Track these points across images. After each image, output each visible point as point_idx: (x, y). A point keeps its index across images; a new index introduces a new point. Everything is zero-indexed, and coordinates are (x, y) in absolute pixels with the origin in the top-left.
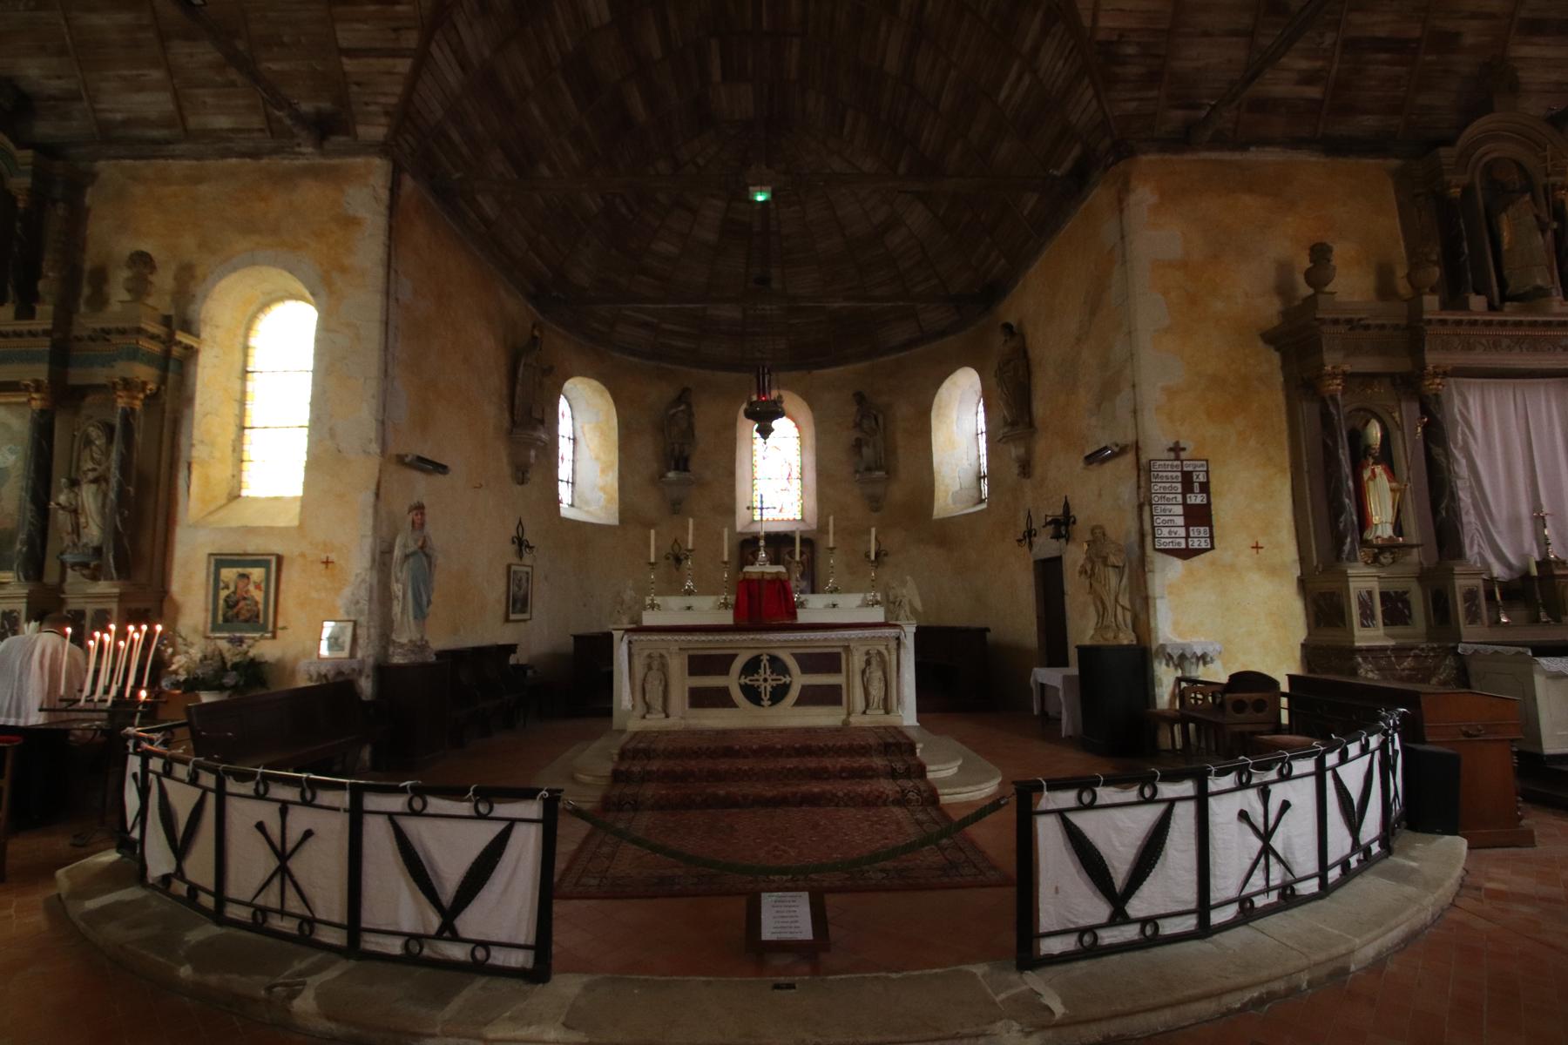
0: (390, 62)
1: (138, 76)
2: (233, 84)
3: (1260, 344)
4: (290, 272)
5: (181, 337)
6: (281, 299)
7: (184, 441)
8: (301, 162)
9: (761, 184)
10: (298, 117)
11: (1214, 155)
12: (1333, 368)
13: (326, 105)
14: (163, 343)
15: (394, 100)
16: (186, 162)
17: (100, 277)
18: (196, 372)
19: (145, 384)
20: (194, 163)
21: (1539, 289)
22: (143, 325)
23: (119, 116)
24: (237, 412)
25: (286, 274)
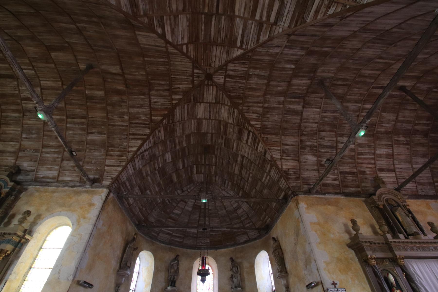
0: (117, 168)
2: (75, 171)
3: (347, 248)
4: (69, 218)
5: (27, 237)
6: (63, 225)
7: (9, 272)
8: (85, 189)
9: (205, 198)
10: (89, 179)
11: (318, 196)
12: (371, 256)
13: (97, 176)
14: (20, 238)
15: (115, 176)
16: (54, 188)
17: (13, 216)
18: (25, 248)
19: (7, 251)
20: (56, 188)
21: (415, 232)
22: (17, 233)
23: (42, 176)
24: (31, 262)
25: (67, 218)
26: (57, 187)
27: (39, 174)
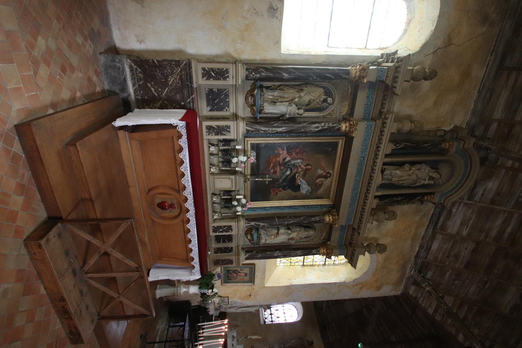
0: (434, 307)
1: (467, 226)
15: (420, 302)
20: (422, 236)
23: (454, 210)
26: (423, 237)
27: (459, 206)
